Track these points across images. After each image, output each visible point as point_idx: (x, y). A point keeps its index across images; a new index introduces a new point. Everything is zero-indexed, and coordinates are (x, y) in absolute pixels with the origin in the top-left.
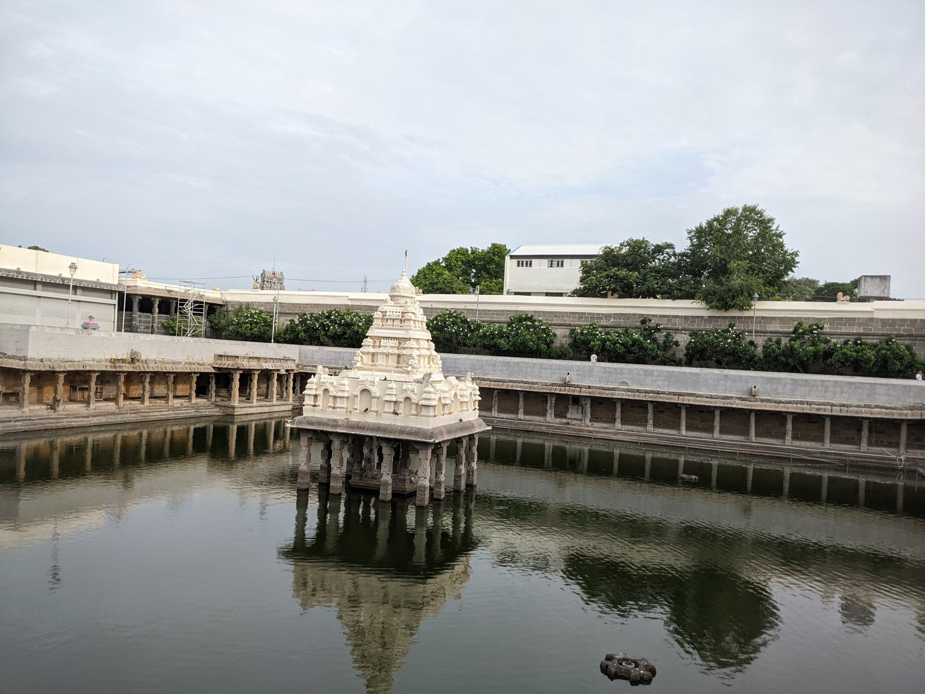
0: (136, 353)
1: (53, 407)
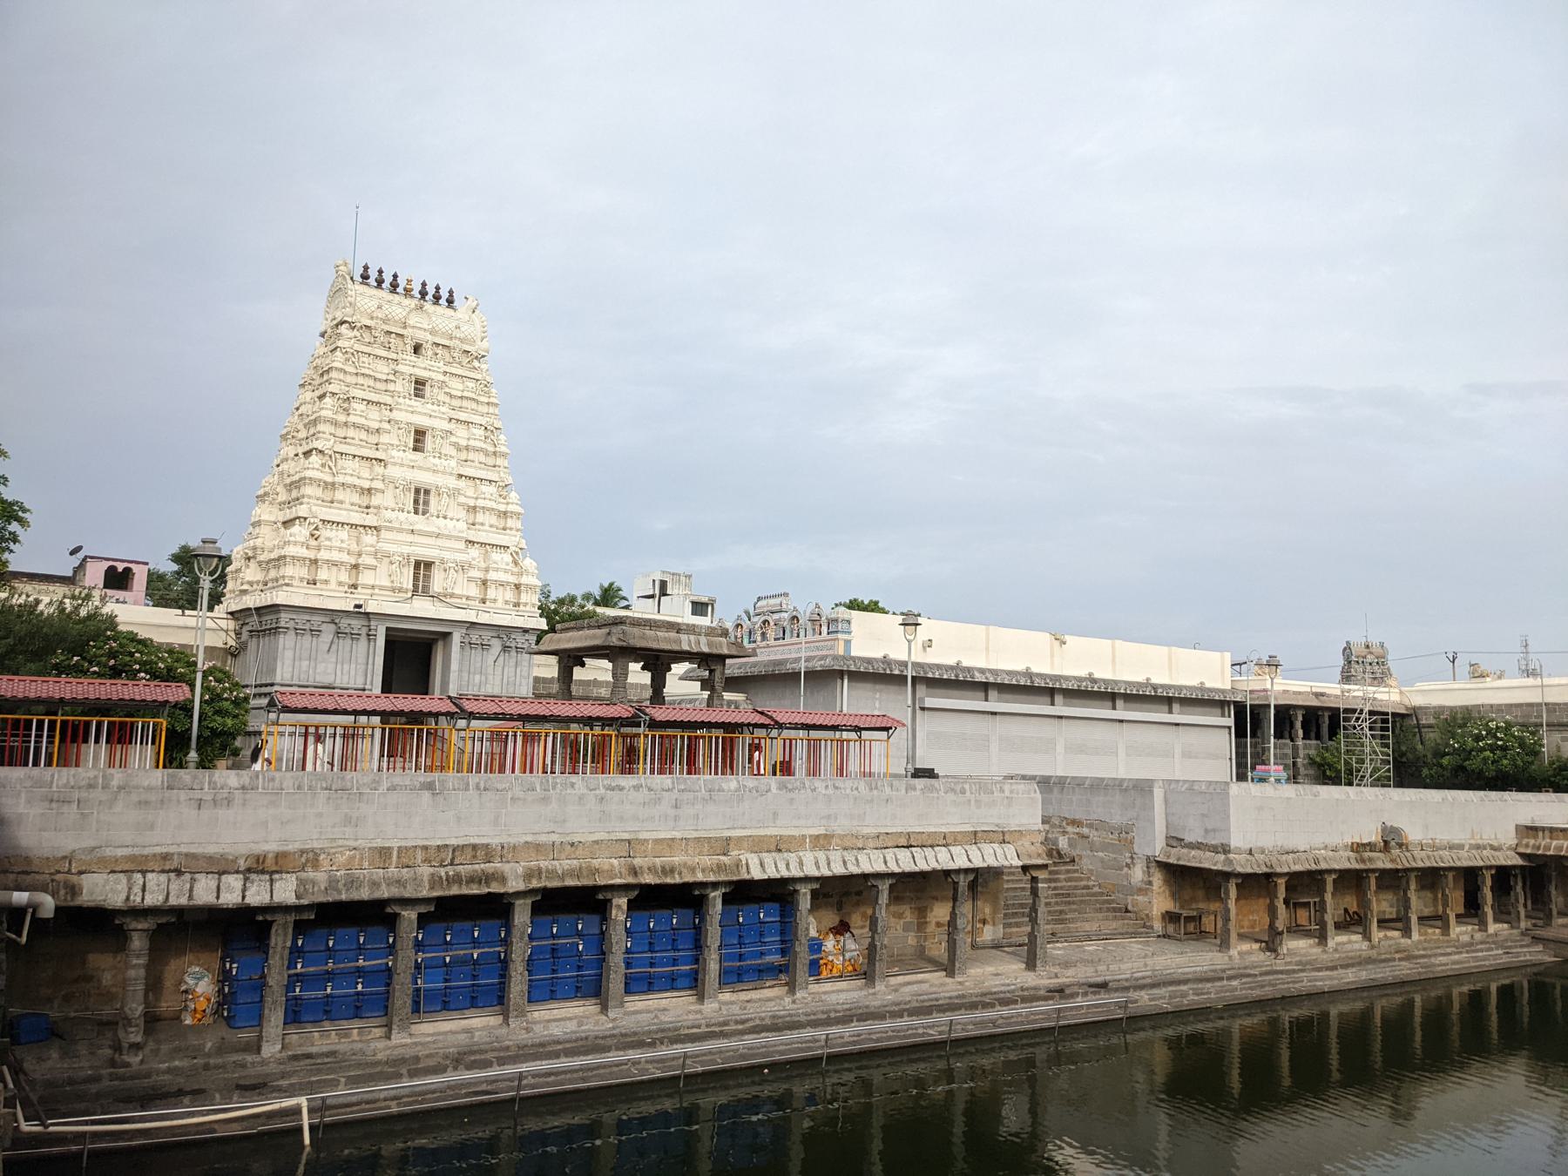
0: (1395, 831)
1: (1271, 943)
